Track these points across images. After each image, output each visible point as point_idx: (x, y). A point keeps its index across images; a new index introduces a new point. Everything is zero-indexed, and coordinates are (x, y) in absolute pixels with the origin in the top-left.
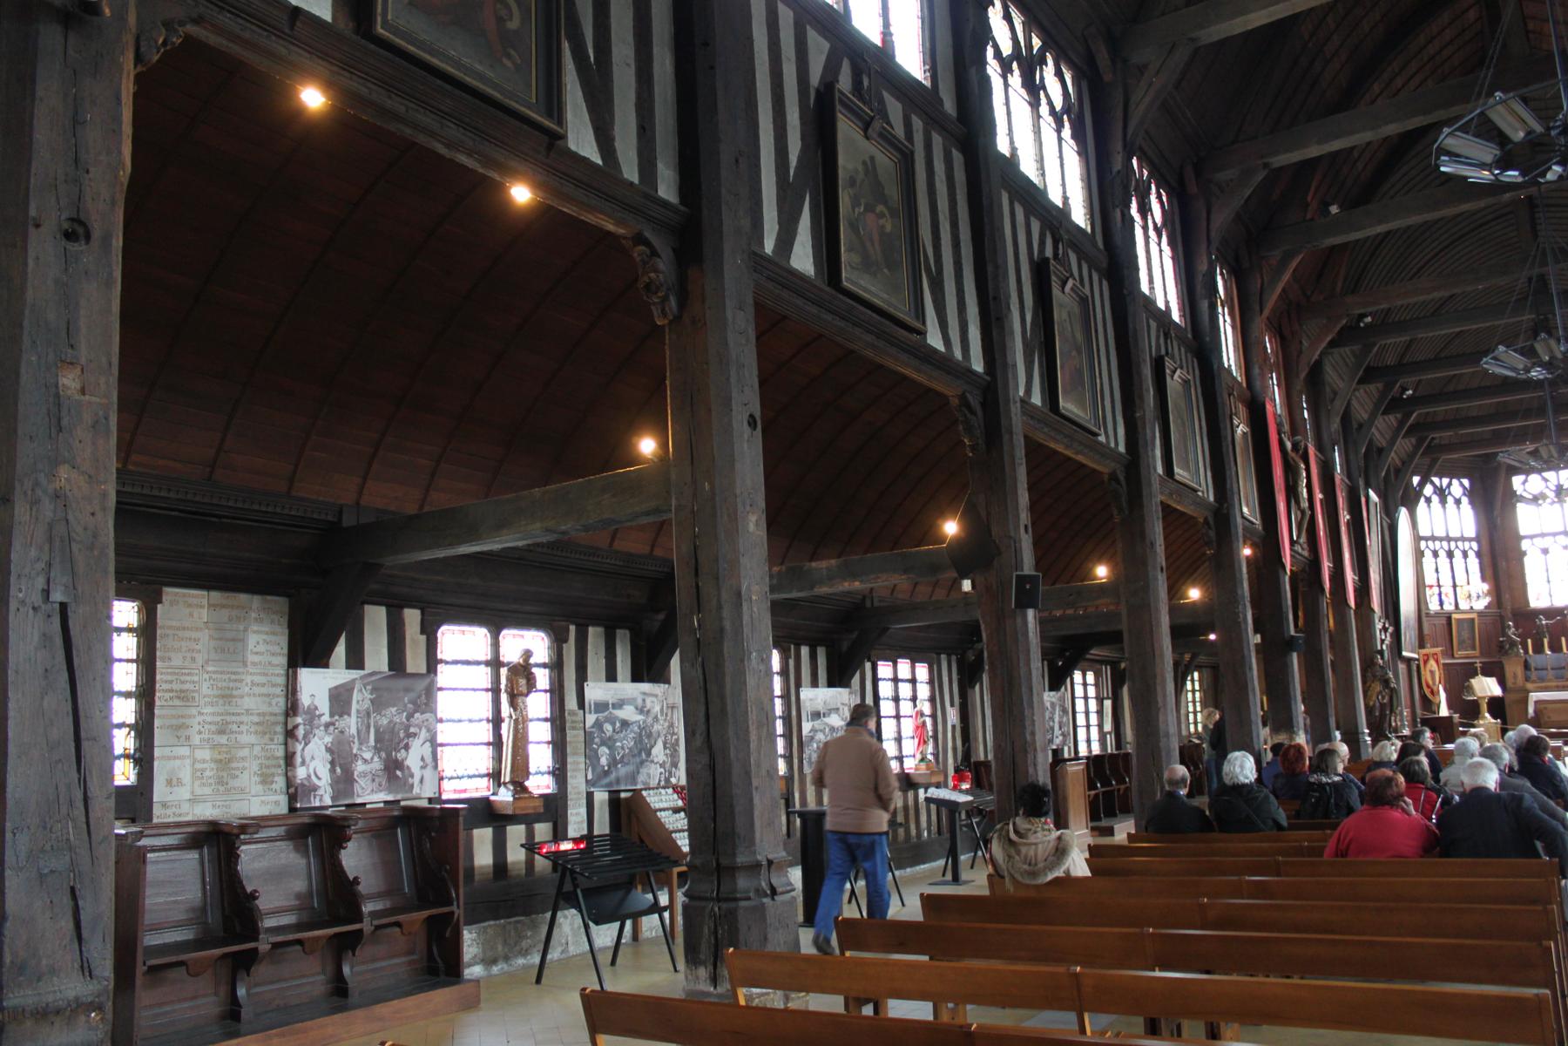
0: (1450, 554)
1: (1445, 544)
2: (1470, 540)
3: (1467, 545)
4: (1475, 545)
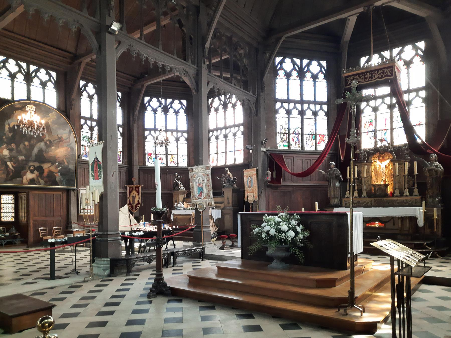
0: (302, 113)
1: (298, 106)
2: (322, 104)
3: (318, 107)
4: (325, 107)
